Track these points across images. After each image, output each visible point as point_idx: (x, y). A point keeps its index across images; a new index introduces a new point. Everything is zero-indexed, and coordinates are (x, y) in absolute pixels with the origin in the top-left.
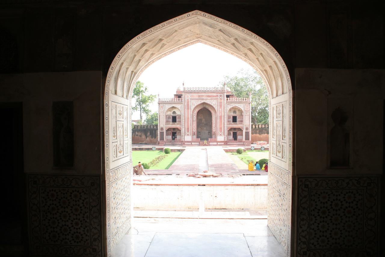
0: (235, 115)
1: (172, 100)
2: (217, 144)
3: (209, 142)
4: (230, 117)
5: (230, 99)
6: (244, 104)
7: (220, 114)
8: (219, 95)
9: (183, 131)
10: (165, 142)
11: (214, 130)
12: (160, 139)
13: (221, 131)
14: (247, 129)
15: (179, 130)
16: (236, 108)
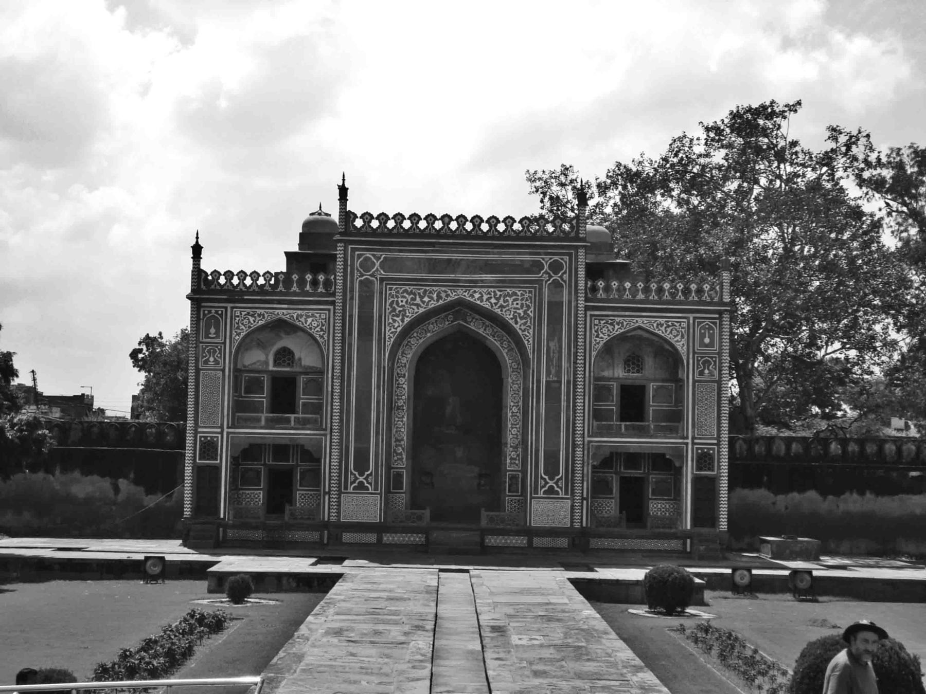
0: (634, 377)
1: (277, 280)
2: (530, 542)
3: (484, 532)
4: (609, 389)
5: (607, 289)
6: (691, 316)
7: (548, 373)
8: (546, 261)
9: (330, 461)
10: (226, 527)
11: (511, 460)
12: (196, 509)
13: (552, 470)
14: (705, 460)
16: (640, 338)
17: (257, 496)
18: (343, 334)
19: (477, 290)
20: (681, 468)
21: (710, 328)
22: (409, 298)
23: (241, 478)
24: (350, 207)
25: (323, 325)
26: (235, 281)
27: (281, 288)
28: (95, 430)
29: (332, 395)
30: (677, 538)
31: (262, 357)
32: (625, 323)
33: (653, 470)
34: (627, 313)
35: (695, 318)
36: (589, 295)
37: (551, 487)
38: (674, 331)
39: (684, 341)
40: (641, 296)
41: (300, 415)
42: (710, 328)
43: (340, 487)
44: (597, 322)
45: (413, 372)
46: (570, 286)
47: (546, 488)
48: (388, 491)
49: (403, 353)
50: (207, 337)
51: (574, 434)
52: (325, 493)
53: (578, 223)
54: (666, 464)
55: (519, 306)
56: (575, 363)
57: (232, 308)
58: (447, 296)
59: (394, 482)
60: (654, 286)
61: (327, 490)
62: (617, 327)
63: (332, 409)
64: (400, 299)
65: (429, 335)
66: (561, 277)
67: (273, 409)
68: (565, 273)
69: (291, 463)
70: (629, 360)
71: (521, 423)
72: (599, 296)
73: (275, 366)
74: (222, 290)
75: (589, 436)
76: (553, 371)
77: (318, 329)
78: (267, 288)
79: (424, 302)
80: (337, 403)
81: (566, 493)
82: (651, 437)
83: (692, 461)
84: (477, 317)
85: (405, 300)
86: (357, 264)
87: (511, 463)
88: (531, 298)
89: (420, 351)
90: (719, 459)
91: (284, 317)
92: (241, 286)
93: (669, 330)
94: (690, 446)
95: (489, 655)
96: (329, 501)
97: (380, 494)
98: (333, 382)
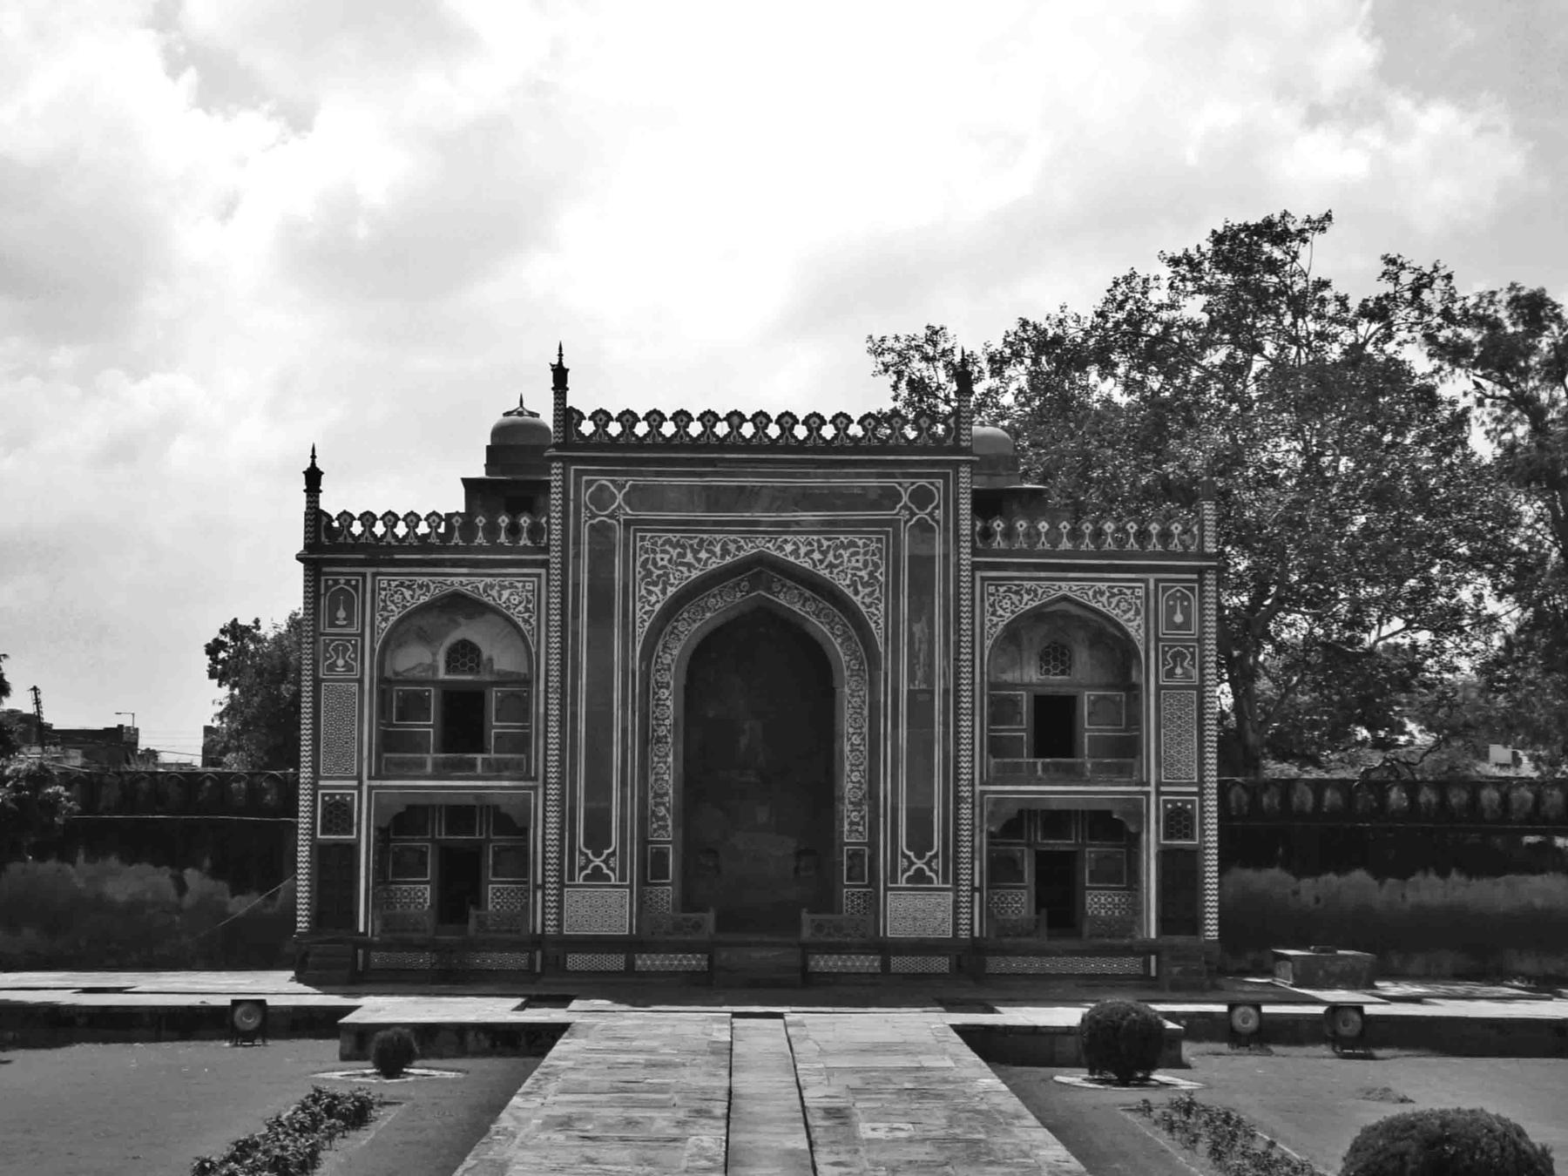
1: (449, 527)
2: (885, 965)
3: (807, 949)
4: (1014, 703)
5: (1009, 533)
6: (1152, 577)
7: (911, 679)
8: (905, 487)
9: (544, 832)
10: (368, 946)
11: (850, 826)
12: (317, 918)
13: (920, 842)
14: (1179, 821)
15: (511, 825)
16: (1065, 616)
17: (421, 894)
18: (563, 614)
19: (789, 538)
20: (1138, 836)
21: (1185, 597)
22: (674, 553)
24: (572, 401)
25: (529, 602)
26: (379, 529)
27: (457, 540)
28: (144, 785)
29: (546, 720)
30: (1136, 954)
31: (428, 660)
32: (1040, 591)
33: (1091, 838)
34: (1043, 574)
35: (1157, 581)
36: (979, 545)
37: (920, 870)
38: (1122, 603)
39: (1139, 620)
40: (1066, 545)
41: (493, 755)
42: (1185, 597)
43: (561, 877)
44: (992, 589)
45: (683, 681)
46: (946, 529)
47: (911, 873)
48: (643, 882)
49: (665, 646)
50: (332, 625)
51: (957, 780)
52: (536, 887)
53: (957, 422)
54: (1113, 828)
55: (860, 565)
56: (957, 659)
57: (374, 575)
58: (739, 548)
59: (653, 867)
60: (1087, 528)
61: (539, 881)
62: (1026, 597)
63: (546, 743)
64: (658, 556)
65: (708, 615)
66: (931, 514)
67: (447, 744)
68: (937, 507)
69: (477, 837)
70: (1048, 654)
71: (866, 763)
72: (995, 545)
73: (449, 670)
74: (357, 544)
75: (982, 783)
76: (920, 674)
77: (520, 608)
78: (433, 540)
79: (699, 560)
80: (554, 734)
81: (945, 881)
82: (1088, 783)
83: (1157, 822)
84: (789, 583)
85: (667, 557)
86: (586, 496)
87: (850, 831)
88: (880, 550)
89: (694, 643)
90: (1202, 818)
91: (462, 589)
92: (389, 538)
93: (1114, 601)
94: (1153, 798)
95: (822, 1157)
96: (544, 901)
97: (630, 887)
98: (547, 698)
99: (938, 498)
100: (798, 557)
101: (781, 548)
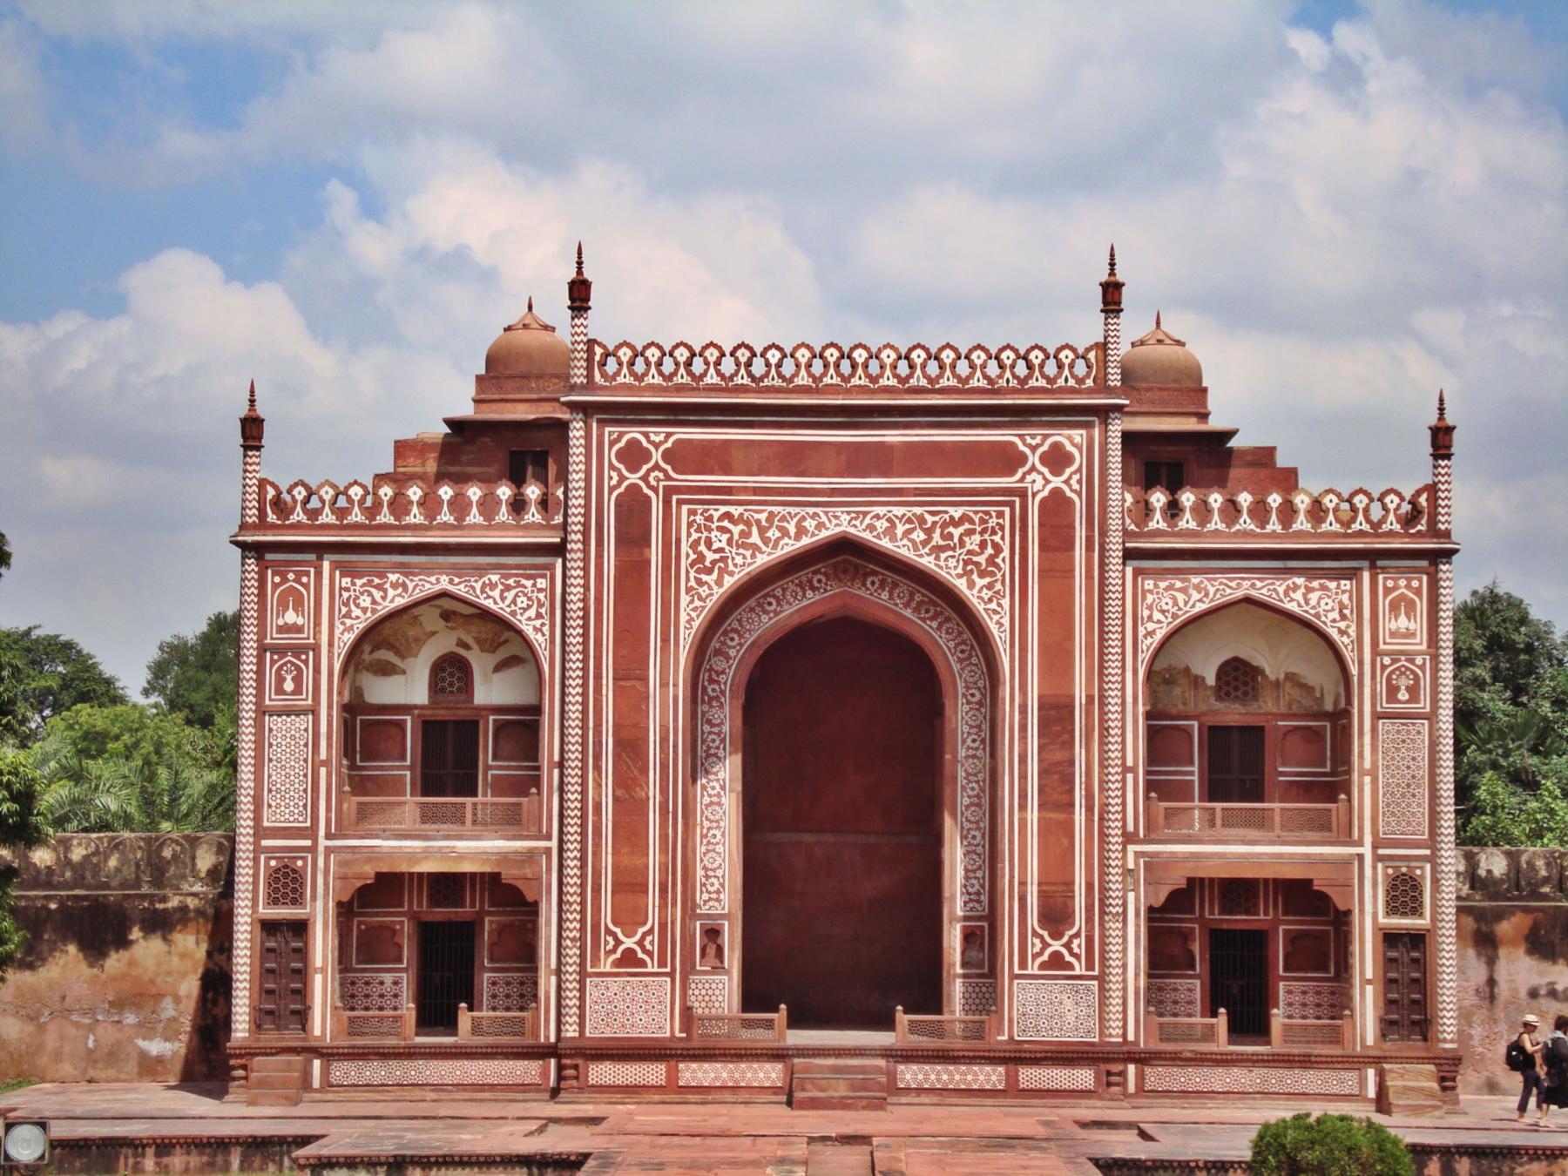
2: (1012, 1079)
4: (1187, 732)
10: (328, 1055)
13: (1055, 916)
14: (1403, 894)
17: (398, 984)
20: (1348, 913)
22: (736, 530)
23: (362, 946)
33: (1286, 913)
37: (1056, 956)
47: (1045, 957)
60: (1275, 500)
81: (1090, 967)
85: (725, 537)
88: (1002, 528)
97: (672, 975)
99: (1079, 459)
100: (893, 539)
101: (871, 528)
